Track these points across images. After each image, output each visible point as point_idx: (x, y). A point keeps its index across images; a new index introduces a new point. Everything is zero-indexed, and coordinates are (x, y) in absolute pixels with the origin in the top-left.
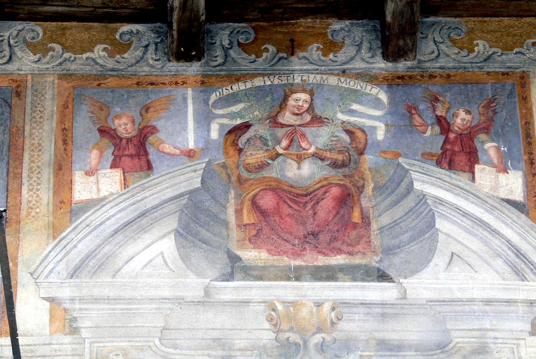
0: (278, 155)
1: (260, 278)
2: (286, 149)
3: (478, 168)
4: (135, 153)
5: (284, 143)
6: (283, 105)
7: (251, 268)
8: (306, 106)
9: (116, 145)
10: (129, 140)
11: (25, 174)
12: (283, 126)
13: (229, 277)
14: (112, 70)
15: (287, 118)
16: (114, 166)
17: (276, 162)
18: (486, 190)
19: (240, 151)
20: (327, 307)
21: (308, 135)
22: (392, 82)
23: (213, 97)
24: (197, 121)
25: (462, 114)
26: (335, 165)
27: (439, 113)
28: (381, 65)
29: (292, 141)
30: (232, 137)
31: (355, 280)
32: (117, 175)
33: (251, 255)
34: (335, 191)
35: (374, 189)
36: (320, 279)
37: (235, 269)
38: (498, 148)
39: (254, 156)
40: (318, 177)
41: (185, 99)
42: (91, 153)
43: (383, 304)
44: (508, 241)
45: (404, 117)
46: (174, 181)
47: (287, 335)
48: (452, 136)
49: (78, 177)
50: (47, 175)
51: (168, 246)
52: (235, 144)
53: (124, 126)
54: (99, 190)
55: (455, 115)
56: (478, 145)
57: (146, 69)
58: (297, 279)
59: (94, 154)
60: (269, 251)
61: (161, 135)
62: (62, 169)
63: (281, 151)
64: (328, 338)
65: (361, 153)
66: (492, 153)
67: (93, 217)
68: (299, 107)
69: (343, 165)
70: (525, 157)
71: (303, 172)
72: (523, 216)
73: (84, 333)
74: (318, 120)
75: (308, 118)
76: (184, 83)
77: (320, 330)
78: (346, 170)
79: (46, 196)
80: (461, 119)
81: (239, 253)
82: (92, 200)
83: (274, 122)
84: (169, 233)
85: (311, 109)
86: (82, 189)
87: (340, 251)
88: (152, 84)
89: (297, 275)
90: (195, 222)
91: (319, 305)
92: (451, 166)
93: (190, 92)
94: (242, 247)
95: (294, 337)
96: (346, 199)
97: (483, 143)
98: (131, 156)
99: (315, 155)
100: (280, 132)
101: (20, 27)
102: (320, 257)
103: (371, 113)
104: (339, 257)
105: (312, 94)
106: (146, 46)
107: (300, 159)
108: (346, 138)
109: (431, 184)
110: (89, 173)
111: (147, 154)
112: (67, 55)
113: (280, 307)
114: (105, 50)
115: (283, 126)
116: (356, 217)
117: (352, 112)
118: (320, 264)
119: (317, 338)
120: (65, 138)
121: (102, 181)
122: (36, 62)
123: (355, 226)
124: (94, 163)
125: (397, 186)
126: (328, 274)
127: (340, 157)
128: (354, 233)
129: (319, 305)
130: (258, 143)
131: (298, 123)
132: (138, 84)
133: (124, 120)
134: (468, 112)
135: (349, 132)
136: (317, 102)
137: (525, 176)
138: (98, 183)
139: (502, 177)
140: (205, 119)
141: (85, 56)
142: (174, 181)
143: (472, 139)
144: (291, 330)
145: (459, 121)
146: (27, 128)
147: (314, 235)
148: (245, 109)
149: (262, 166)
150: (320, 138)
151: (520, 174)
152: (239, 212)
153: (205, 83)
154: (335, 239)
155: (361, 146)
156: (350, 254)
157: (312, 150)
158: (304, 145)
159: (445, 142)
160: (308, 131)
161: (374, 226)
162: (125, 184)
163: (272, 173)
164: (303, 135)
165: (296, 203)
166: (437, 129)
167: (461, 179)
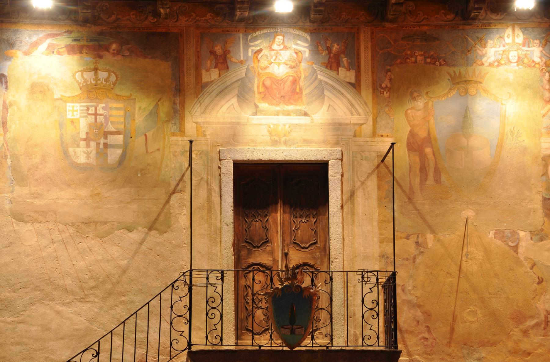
0: (272, 63)
1: (265, 115)
2: (275, 60)
3: (340, 69)
5: (274, 58)
6: (273, 42)
7: (263, 111)
8: (282, 41)
9: (216, 59)
10: (220, 56)
11: (185, 71)
12: (274, 50)
13: (255, 114)
14: (213, 25)
15: (275, 47)
16: (216, 67)
17: (271, 66)
18: (342, 78)
19: (259, 61)
20: (287, 126)
21: (282, 54)
23: (249, 38)
24: (243, 48)
25: (336, 46)
26: (291, 67)
27: (328, 45)
29: (276, 57)
30: (256, 55)
31: (297, 115)
32: (216, 71)
34: (291, 78)
35: (304, 78)
36: (285, 115)
38: (347, 60)
40: (285, 72)
41: (239, 38)
43: (305, 125)
44: (348, 100)
47: (274, 137)
48: (332, 55)
49: (204, 72)
50: (193, 71)
52: (257, 58)
53: (218, 49)
54: (211, 78)
55: (333, 46)
56: (341, 59)
57: (226, 24)
58: (278, 115)
59: (209, 62)
60: (268, 103)
61: (232, 54)
62: (198, 69)
63: (273, 61)
64: (287, 139)
65: (300, 63)
66: (345, 62)
68: (279, 42)
69: (294, 67)
70: (357, 64)
72: (354, 89)
73: (208, 137)
74: (286, 48)
75: (282, 47)
76: (239, 31)
77: (285, 135)
78: (295, 69)
79: (193, 80)
81: (258, 104)
82: (208, 82)
83: (271, 49)
84: (234, 96)
85: (283, 42)
86: (205, 78)
87: (292, 104)
88: (228, 31)
89: (277, 114)
91: (284, 125)
92: (331, 69)
93: (241, 35)
94: (259, 102)
95: (277, 138)
97: (342, 58)
98: (221, 63)
99: (284, 63)
100: (273, 53)
101: (180, 5)
102: (286, 106)
104: (292, 106)
105: (284, 37)
106: (225, 14)
107: (279, 64)
108: (295, 55)
110: (208, 70)
111: (227, 62)
112: (197, 18)
113: (272, 126)
114: (211, 15)
115: (274, 50)
116: (298, 90)
117: (297, 44)
118: (285, 109)
119: (283, 139)
120: (198, 56)
121: (212, 73)
122: (186, 21)
123: (297, 93)
124: (209, 66)
126: (287, 113)
127: (293, 64)
128: (297, 97)
129: (284, 125)
130: (265, 58)
131: (279, 49)
132: (223, 31)
133: (218, 47)
134: (338, 45)
135: (296, 53)
136: (286, 40)
137: (356, 72)
139: (348, 72)
141: (204, 18)
143: (338, 57)
144: (275, 135)
145: (334, 49)
146: (185, 51)
147: (283, 97)
148: (260, 43)
149: (266, 68)
151: (354, 71)
152: (258, 87)
154: (290, 99)
155: (300, 59)
156: (295, 105)
157: (283, 61)
158: (281, 58)
159: (330, 58)
160: (282, 52)
161: (304, 93)
162: (220, 75)
163: (269, 70)
164: (280, 54)
165: (278, 83)
166: (327, 52)
167: (333, 73)
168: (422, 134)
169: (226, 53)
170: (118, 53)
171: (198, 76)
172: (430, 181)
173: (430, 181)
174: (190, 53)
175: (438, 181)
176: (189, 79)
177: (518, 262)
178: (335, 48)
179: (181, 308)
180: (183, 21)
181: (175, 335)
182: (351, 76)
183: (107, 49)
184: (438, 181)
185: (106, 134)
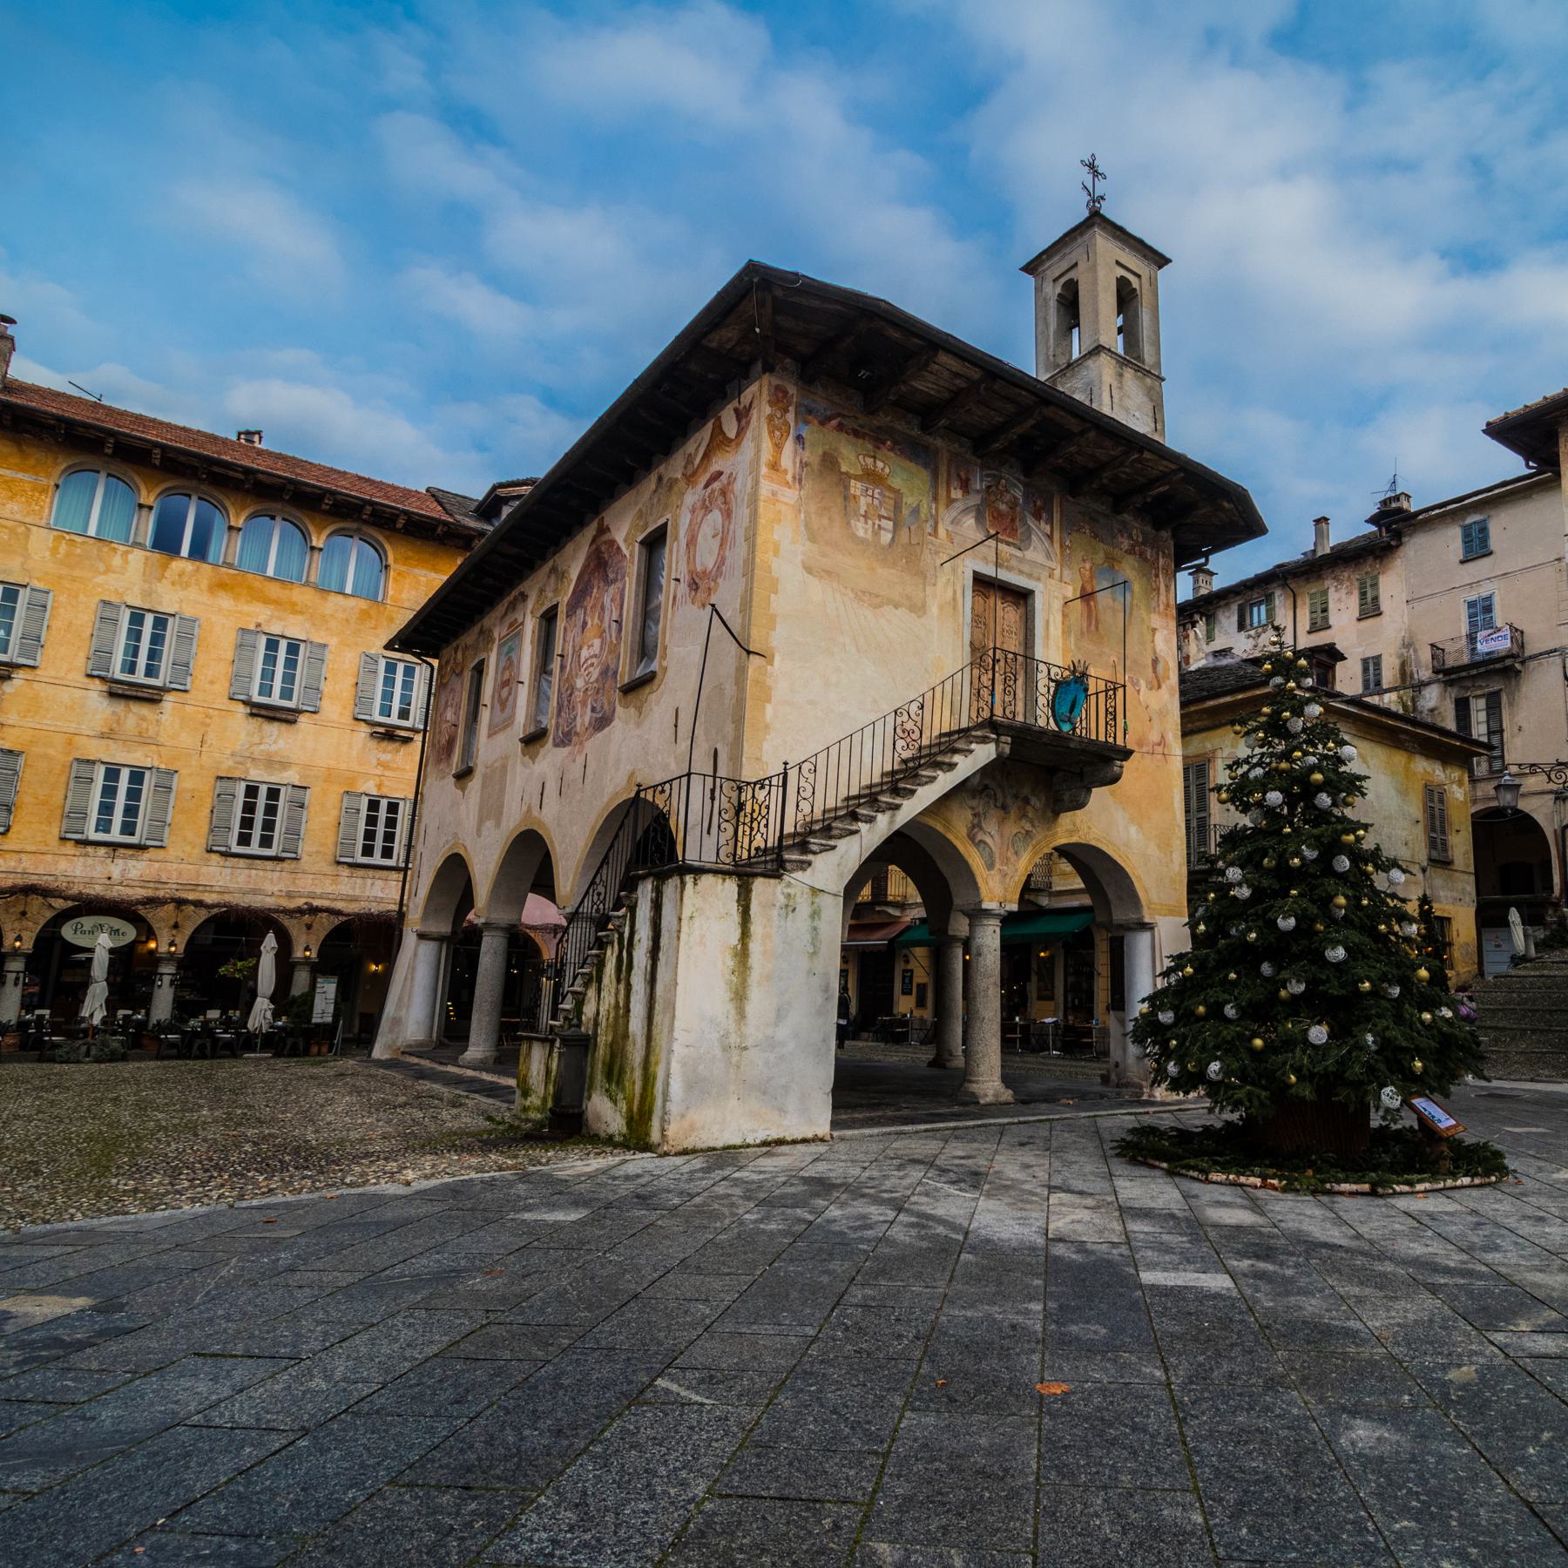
4: (965, 486)
22: (1025, 485)
39: (993, 498)
42: (955, 483)
45: (1026, 496)
67: (956, 505)
71: (1003, 507)
96: (1013, 520)
109: (1031, 522)
120: (949, 474)
138: (957, 494)
142: (975, 500)
150: (1007, 497)
153: (982, 469)
168: (1089, 590)
170: (891, 450)
171: (949, 492)
174: (943, 469)
176: (942, 492)
180: (939, 442)
181: (982, 704)
182: (1048, 529)
183: (884, 443)
185: (881, 517)
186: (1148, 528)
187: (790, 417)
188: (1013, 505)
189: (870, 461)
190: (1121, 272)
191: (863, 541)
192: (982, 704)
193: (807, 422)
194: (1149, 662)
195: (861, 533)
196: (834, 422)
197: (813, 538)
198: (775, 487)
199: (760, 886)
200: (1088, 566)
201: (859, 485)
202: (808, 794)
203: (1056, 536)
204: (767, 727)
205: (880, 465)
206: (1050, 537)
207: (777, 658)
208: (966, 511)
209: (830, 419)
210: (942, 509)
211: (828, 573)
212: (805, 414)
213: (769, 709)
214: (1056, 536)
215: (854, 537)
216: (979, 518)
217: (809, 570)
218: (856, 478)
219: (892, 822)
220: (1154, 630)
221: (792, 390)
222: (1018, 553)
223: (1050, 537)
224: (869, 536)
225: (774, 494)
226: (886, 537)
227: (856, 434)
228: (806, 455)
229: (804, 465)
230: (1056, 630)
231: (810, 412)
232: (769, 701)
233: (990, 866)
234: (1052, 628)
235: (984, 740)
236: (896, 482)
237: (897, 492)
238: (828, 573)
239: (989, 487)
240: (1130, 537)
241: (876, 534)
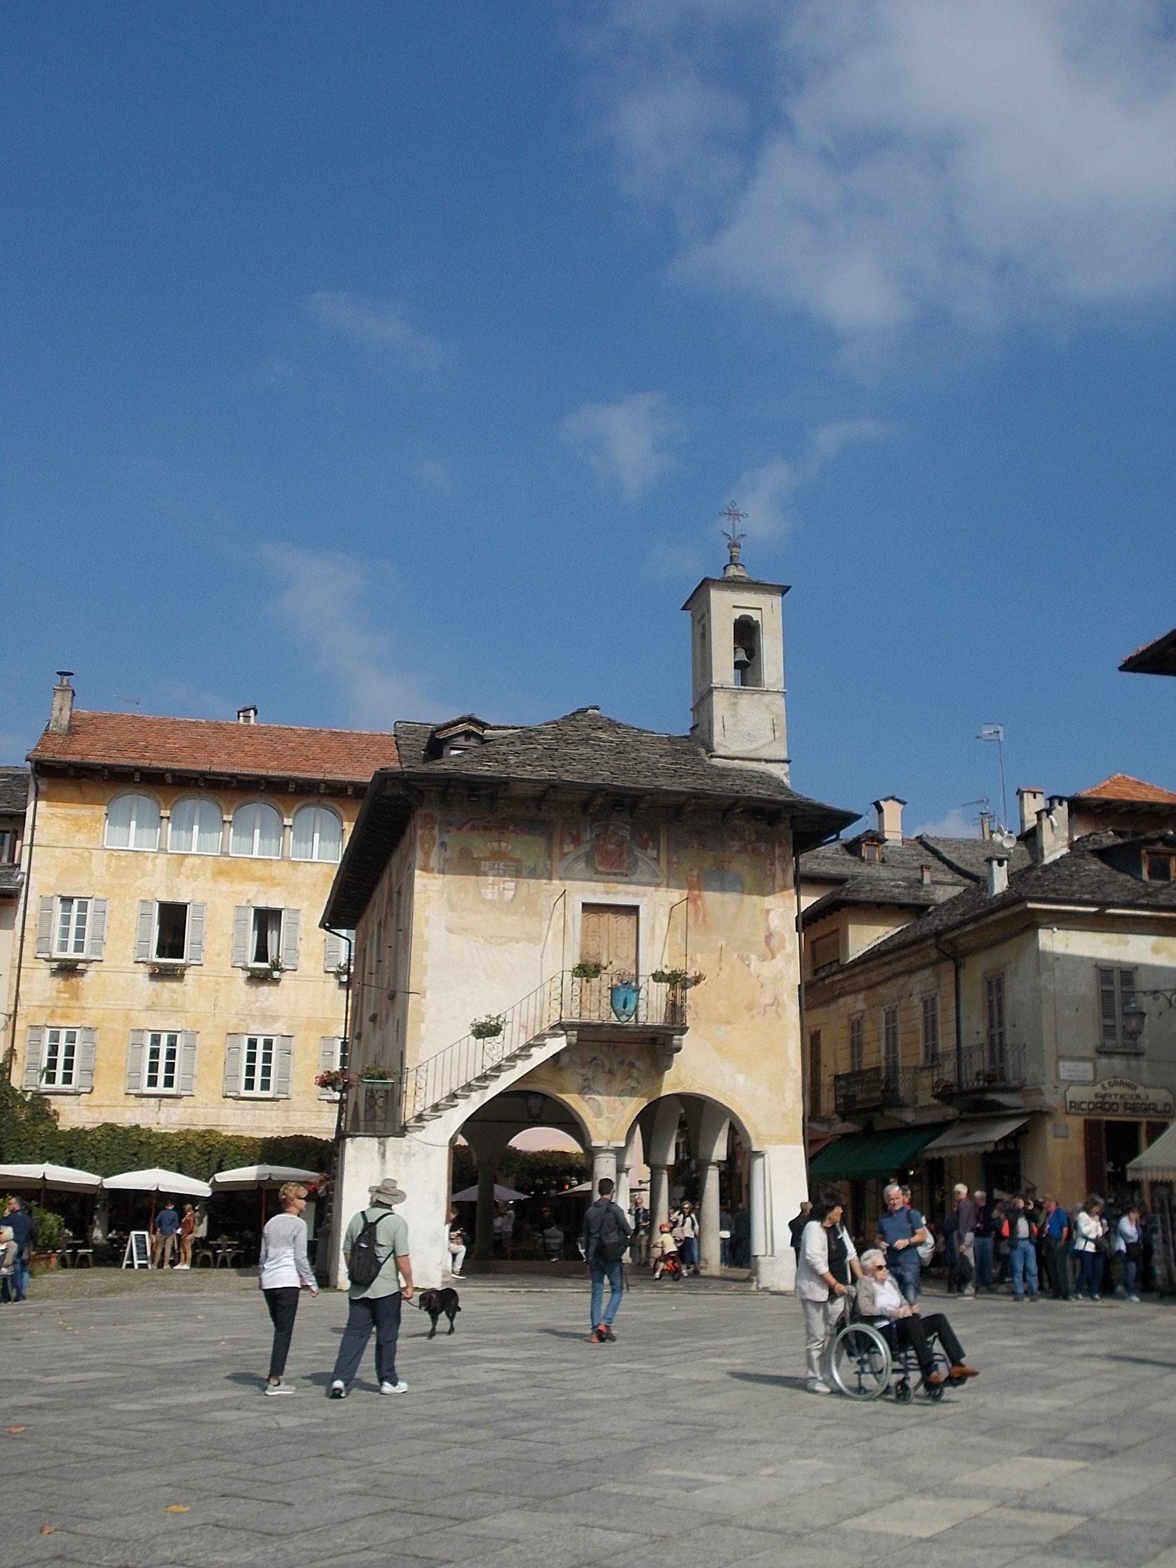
4: (577, 841)
28: (630, 820)
33: (600, 869)
37: (597, 872)
45: (633, 836)
46: (586, 848)
51: (583, 865)
53: (574, 833)
71: (611, 847)
80: (645, 835)
86: (566, 850)
90: (589, 861)
96: (620, 855)
103: (626, 834)
109: (638, 853)
125: (630, 853)
138: (568, 848)
140: (591, 831)
142: (586, 848)
169: (579, 835)
170: (513, 831)
171: (562, 848)
172: (700, 921)
173: (700, 921)
175: (704, 921)
176: (556, 851)
177: (750, 973)
178: (645, 835)
179: (556, 995)
181: (552, 1011)
182: (654, 853)
184: (704, 921)
186: (763, 826)
187: (436, 831)
188: (620, 844)
189: (495, 845)
190: (738, 614)
191: (492, 902)
192: (552, 1011)
193: (448, 832)
194: (763, 937)
195: (489, 897)
196: (468, 826)
197: (453, 908)
198: (425, 881)
199: (391, 1141)
200: (695, 873)
201: (487, 863)
202: (423, 1084)
203: (663, 856)
204: (422, 1038)
205: (504, 844)
206: (657, 860)
207: (428, 992)
208: (576, 859)
209: (464, 824)
210: (556, 863)
211: (465, 929)
212: (447, 825)
213: (423, 1026)
214: (663, 856)
215: (485, 901)
216: (587, 863)
217: (450, 930)
218: (486, 859)
219: (482, 1097)
220: (768, 911)
221: (437, 813)
222: (626, 879)
223: (657, 860)
224: (496, 897)
225: (425, 886)
226: (509, 895)
227: (485, 828)
228: (448, 854)
229: (446, 861)
230: (661, 931)
231: (450, 824)
232: (423, 1021)
233: (599, 1114)
234: (658, 931)
235: (555, 1035)
236: (517, 854)
237: (518, 861)
238: (465, 929)
239: (597, 836)
240: (742, 839)
241: (501, 894)
